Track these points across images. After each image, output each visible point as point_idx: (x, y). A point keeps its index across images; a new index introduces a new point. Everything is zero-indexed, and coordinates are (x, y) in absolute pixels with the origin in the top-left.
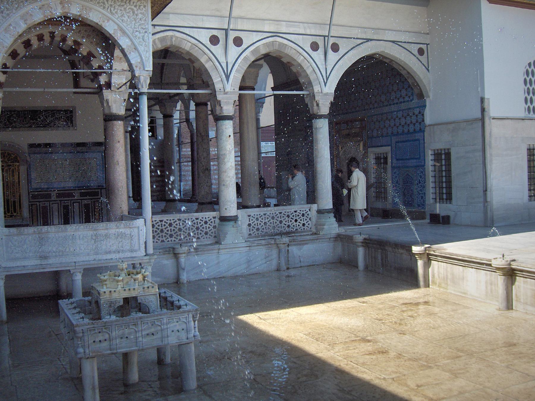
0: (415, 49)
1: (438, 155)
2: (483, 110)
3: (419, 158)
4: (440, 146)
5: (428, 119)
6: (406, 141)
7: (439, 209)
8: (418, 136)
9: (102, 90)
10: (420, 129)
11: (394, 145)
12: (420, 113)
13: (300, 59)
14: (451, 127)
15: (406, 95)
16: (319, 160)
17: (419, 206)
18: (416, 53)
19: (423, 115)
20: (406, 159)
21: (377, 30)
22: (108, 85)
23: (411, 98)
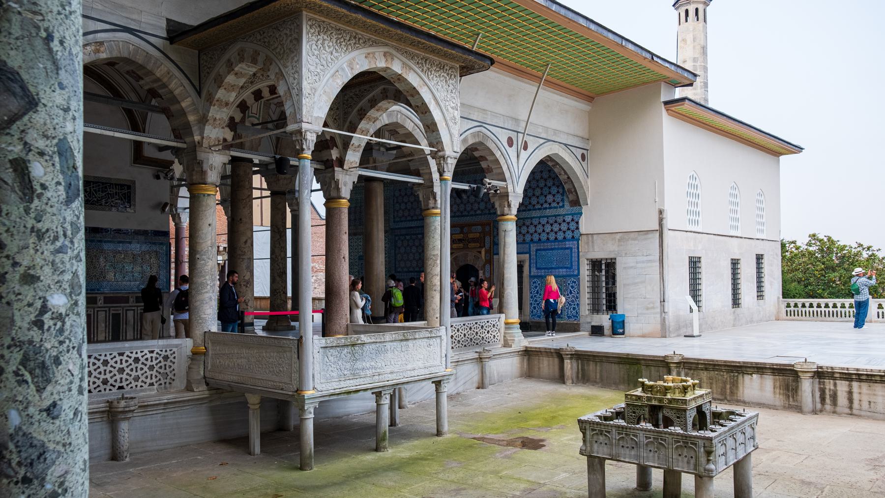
0: (579, 153)
1: (595, 264)
2: (661, 220)
3: (571, 268)
4: (599, 254)
5: (584, 228)
6: (552, 249)
7: (604, 320)
8: (568, 244)
9: (332, 167)
10: (573, 237)
11: (533, 253)
12: (573, 220)
13: (498, 155)
14: (618, 236)
15: (554, 201)
16: (506, 266)
17: (569, 317)
18: (580, 158)
19: (577, 223)
20: (552, 268)
21: (556, 132)
22: (341, 162)
23: (561, 204)
